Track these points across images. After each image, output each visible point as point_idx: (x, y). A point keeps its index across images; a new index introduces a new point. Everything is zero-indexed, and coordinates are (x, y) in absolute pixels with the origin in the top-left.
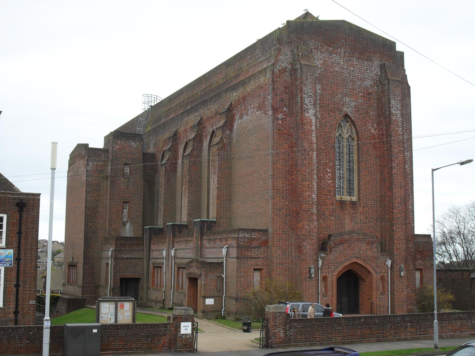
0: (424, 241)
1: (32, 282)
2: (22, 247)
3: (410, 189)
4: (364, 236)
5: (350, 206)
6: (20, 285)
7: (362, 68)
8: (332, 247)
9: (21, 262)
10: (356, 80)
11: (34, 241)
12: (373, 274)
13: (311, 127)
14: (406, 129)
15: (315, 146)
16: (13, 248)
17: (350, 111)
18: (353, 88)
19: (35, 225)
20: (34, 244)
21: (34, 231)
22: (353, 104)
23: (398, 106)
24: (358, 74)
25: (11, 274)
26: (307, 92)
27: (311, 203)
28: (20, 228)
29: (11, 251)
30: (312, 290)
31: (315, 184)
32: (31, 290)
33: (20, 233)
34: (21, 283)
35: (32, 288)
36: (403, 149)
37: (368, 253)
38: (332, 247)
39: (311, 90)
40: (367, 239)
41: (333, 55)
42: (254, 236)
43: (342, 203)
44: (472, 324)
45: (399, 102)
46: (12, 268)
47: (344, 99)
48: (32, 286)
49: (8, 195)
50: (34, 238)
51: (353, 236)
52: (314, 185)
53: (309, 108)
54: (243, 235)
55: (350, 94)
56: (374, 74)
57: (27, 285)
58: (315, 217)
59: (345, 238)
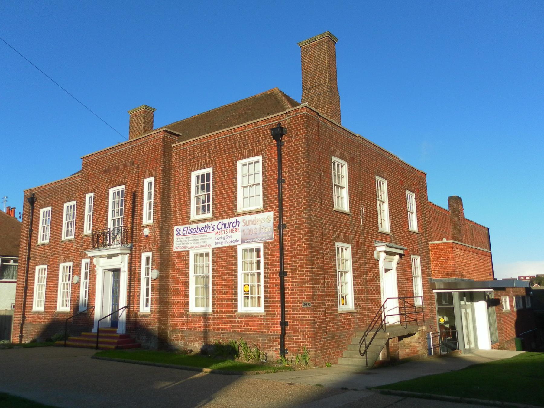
1: (303, 266)
2: (285, 204)
6: (286, 272)
9: (286, 231)
11: (302, 190)
16: (273, 208)
19: (301, 161)
20: (302, 195)
21: (300, 173)
25: (273, 255)
28: (280, 173)
29: (271, 214)
32: (303, 282)
33: (280, 181)
34: (287, 269)
35: (303, 276)
46: (274, 243)
48: (305, 274)
49: (261, 124)
50: (302, 185)
57: (296, 271)
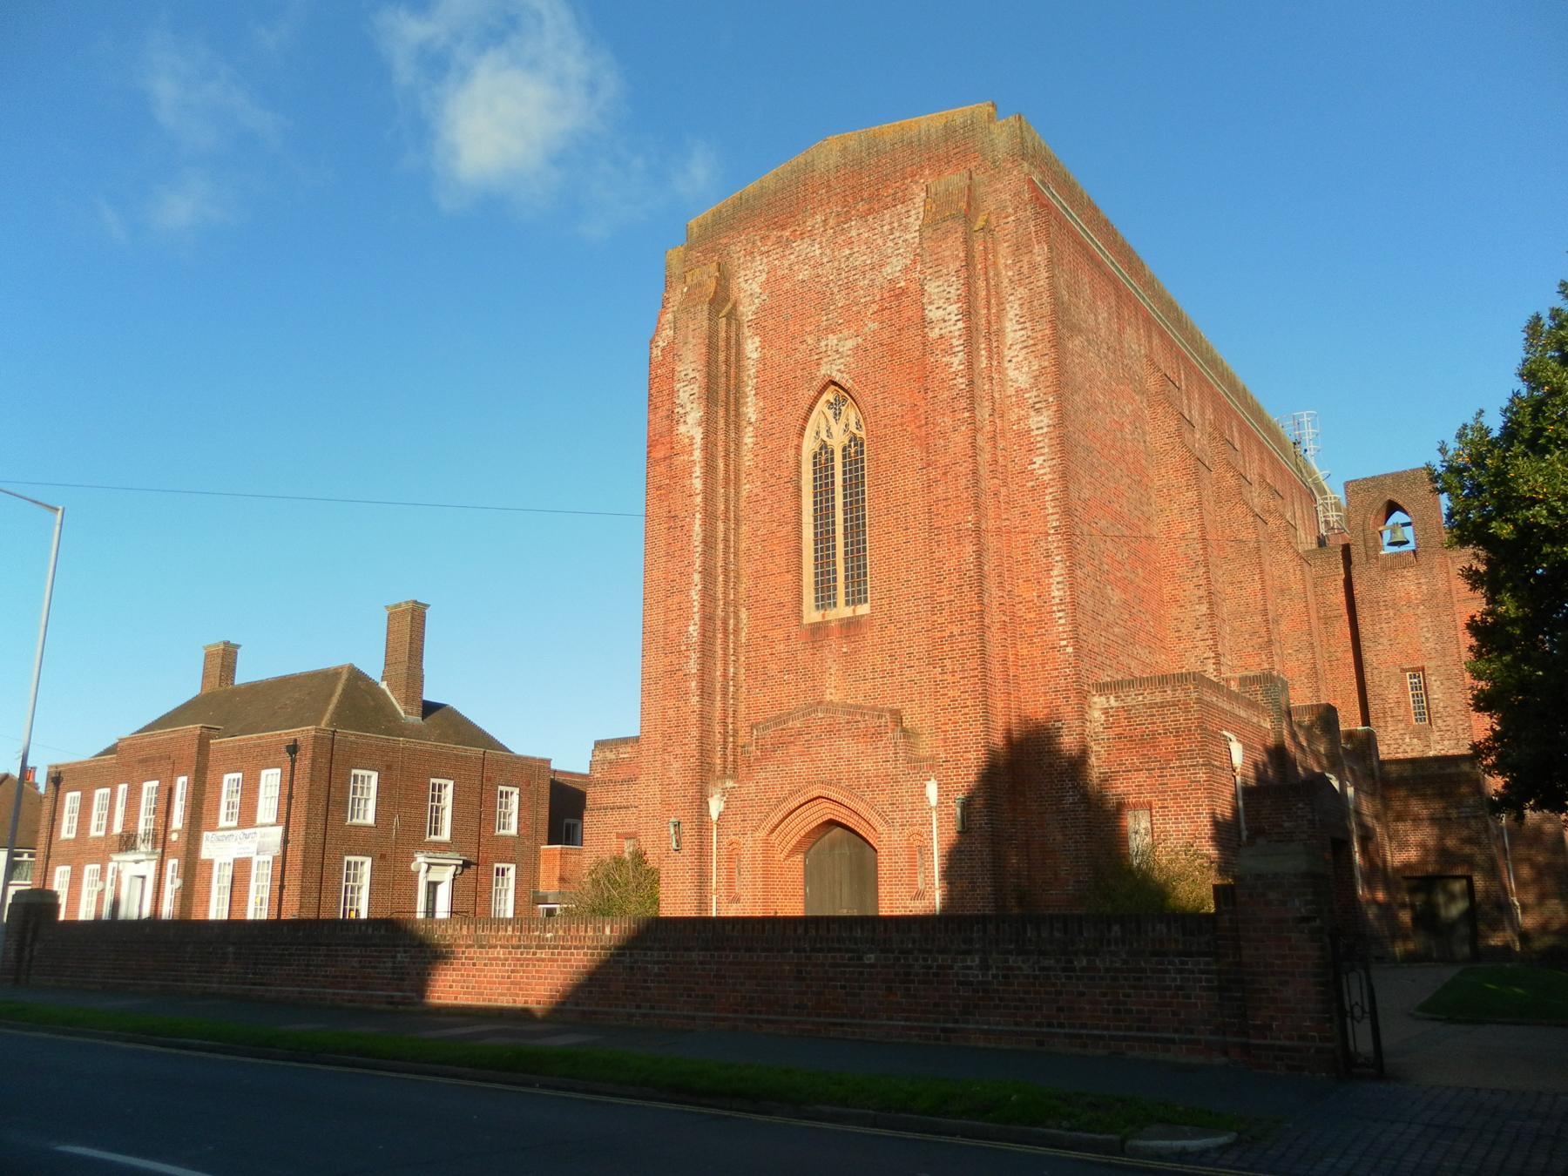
0: (1158, 700)
3: (1052, 531)
4: (849, 713)
5: (841, 633)
7: (875, 237)
8: (752, 759)
10: (857, 277)
12: (880, 829)
13: (692, 455)
14: (1031, 342)
15: (699, 499)
17: (839, 367)
18: (847, 302)
22: (850, 344)
23: (949, 292)
24: (865, 257)
26: (685, 373)
27: (684, 648)
30: (682, 883)
31: (695, 597)
36: (967, 414)
37: (864, 766)
38: (752, 759)
39: (693, 366)
40: (859, 721)
41: (794, 245)
42: (625, 753)
43: (818, 630)
44: (394, 963)
45: (954, 279)
47: (823, 343)
51: (815, 719)
52: (694, 601)
53: (688, 409)
54: (601, 755)
55: (840, 321)
56: (915, 231)
58: (693, 684)
59: (792, 728)
